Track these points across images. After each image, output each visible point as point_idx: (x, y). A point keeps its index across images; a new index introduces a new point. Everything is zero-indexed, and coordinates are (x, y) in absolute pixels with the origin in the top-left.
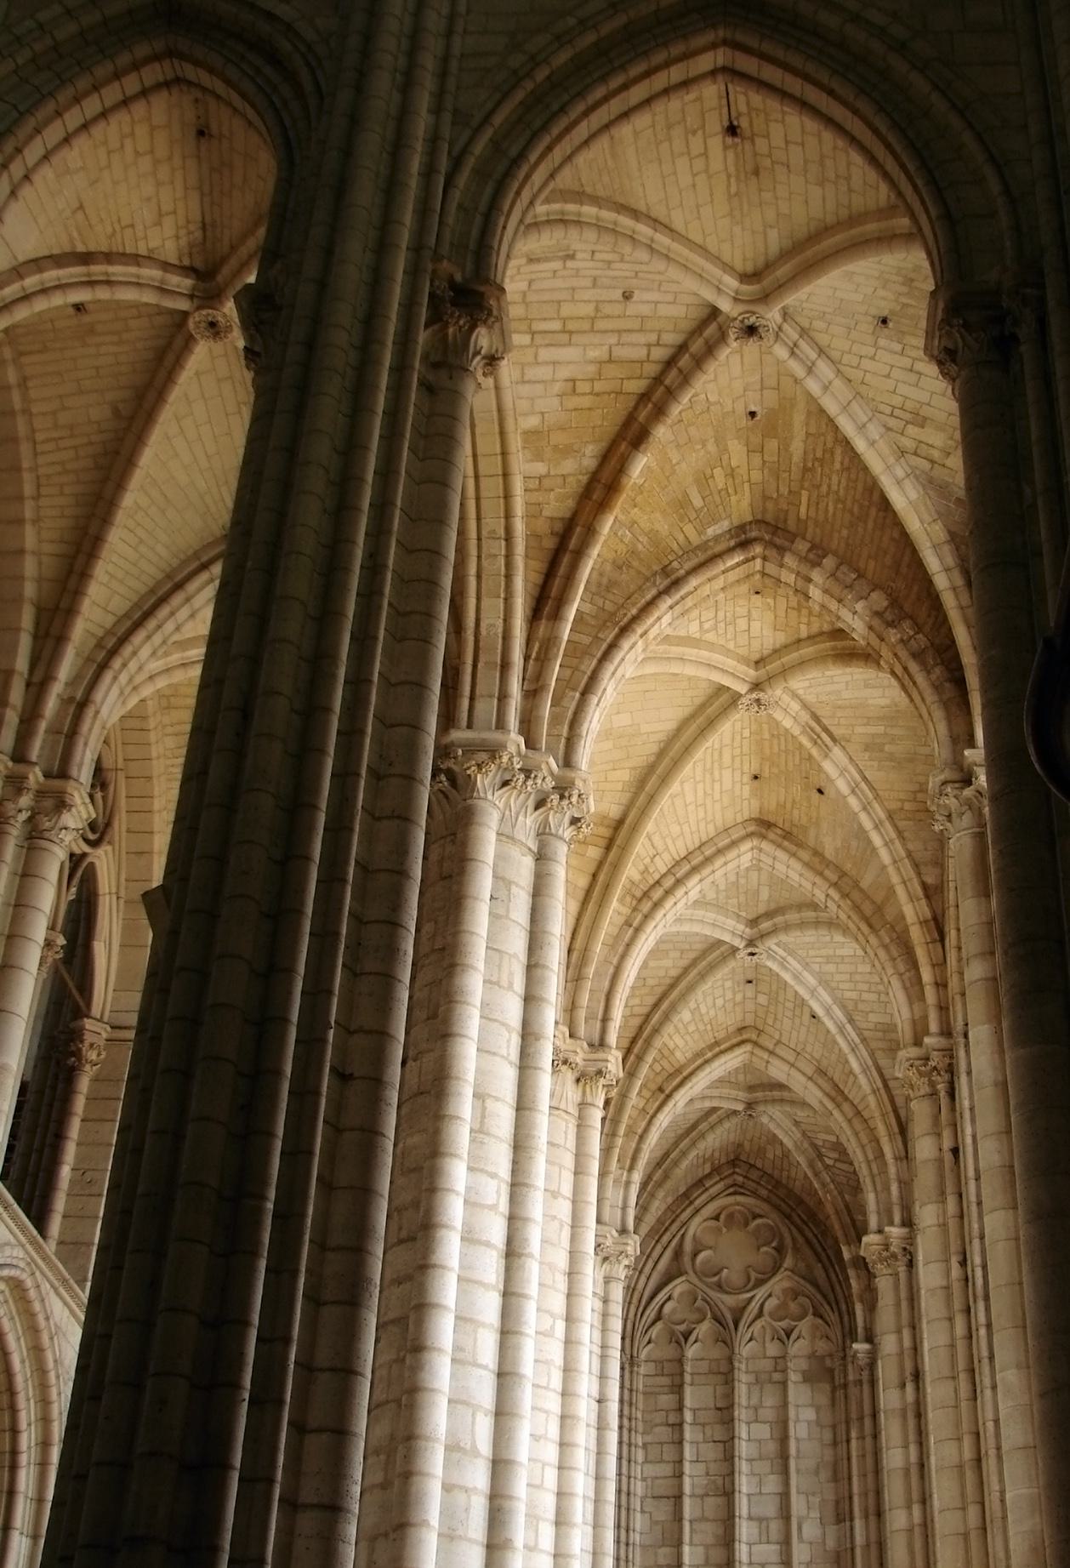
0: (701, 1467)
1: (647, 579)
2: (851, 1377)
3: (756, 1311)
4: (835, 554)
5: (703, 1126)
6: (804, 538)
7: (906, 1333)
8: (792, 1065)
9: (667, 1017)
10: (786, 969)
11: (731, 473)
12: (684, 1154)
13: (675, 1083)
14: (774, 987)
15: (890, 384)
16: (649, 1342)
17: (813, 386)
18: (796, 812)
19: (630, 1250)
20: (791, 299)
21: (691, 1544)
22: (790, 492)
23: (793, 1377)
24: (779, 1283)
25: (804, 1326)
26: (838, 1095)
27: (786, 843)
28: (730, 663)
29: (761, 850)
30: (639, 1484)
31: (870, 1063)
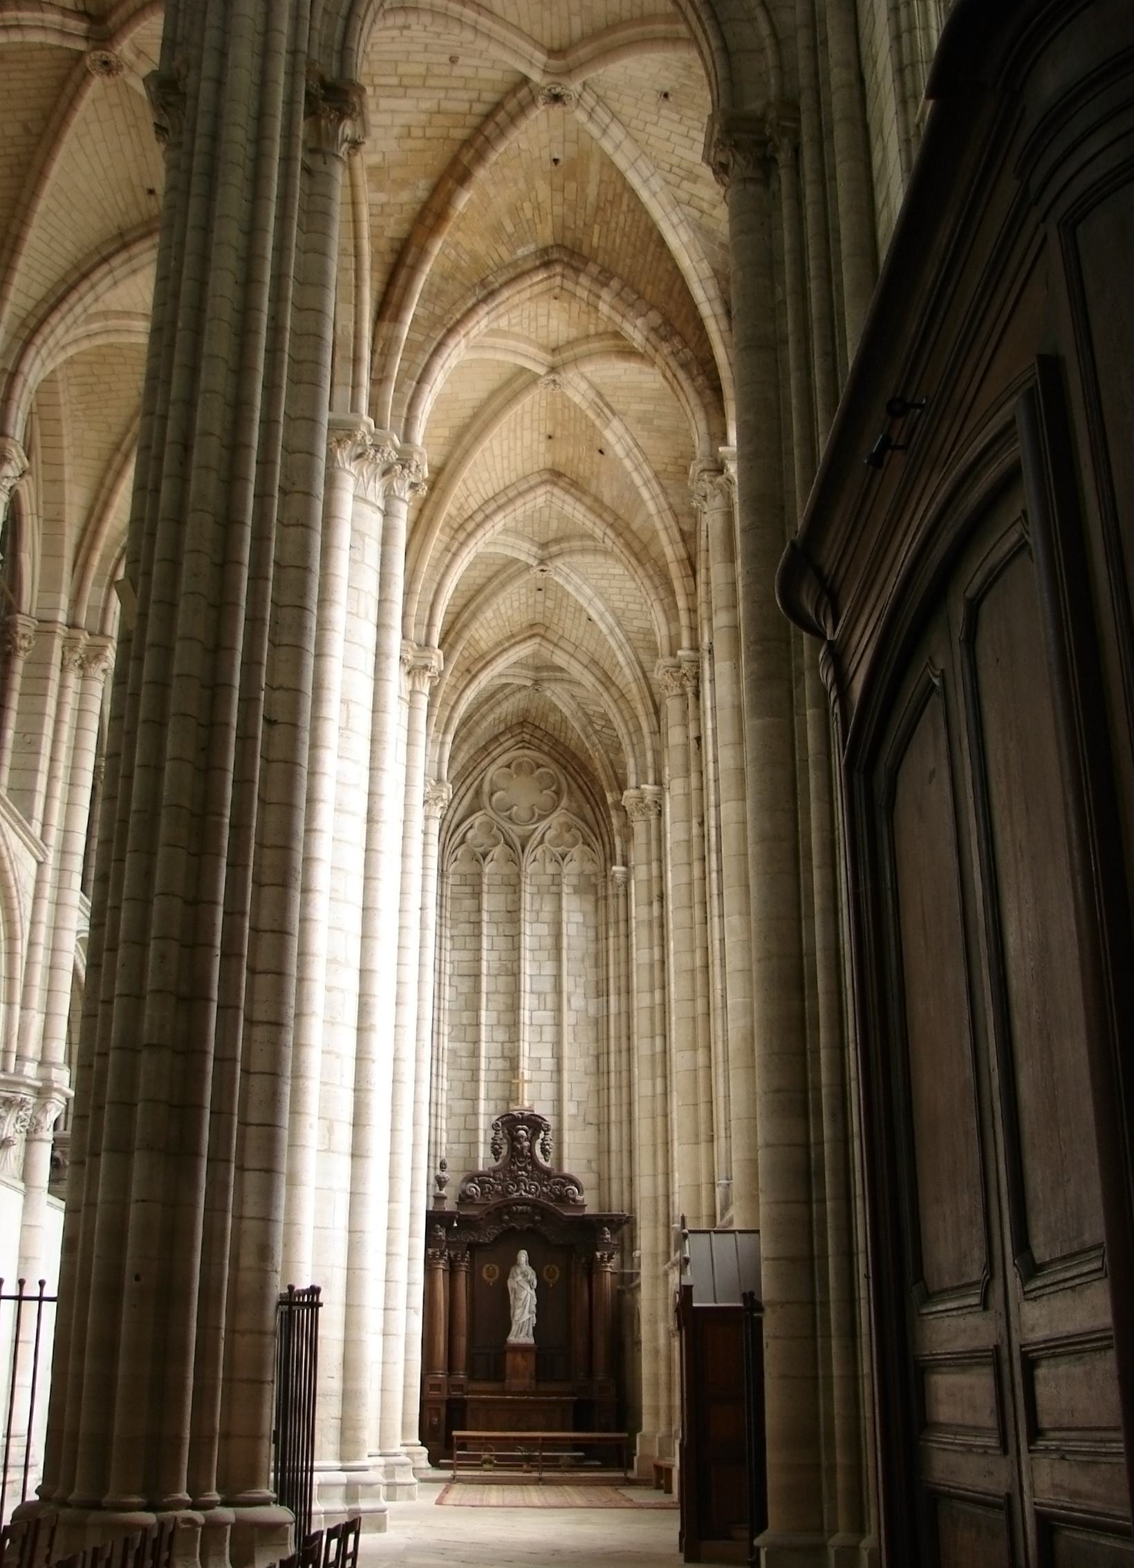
0: (495, 955)
1: (469, 289)
2: (610, 892)
3: (538, 839)
4: (621, 278)
5: (500, 696)
6: (595, 263)
8: (572, 656)
9: (474, 616)
10: (569, 582)
11: (538, 207)
12: (484, 717)
13: (481, 665)
14: (560, 595)
15: (669, 147)
16: (455, 860)
17: (608, 146)
18: (581, 467)
19: (445, 796)
20: (590, 75)
21: (487, 1010)
22: (585, 224)
23: (566, 889)
24: (557, 819)
25: (576, 852)
26: (607, 681)
27: (573, 490)
28: (532, 351)
29: (553, 494)
30: (448, 965)
31: (633, 658)
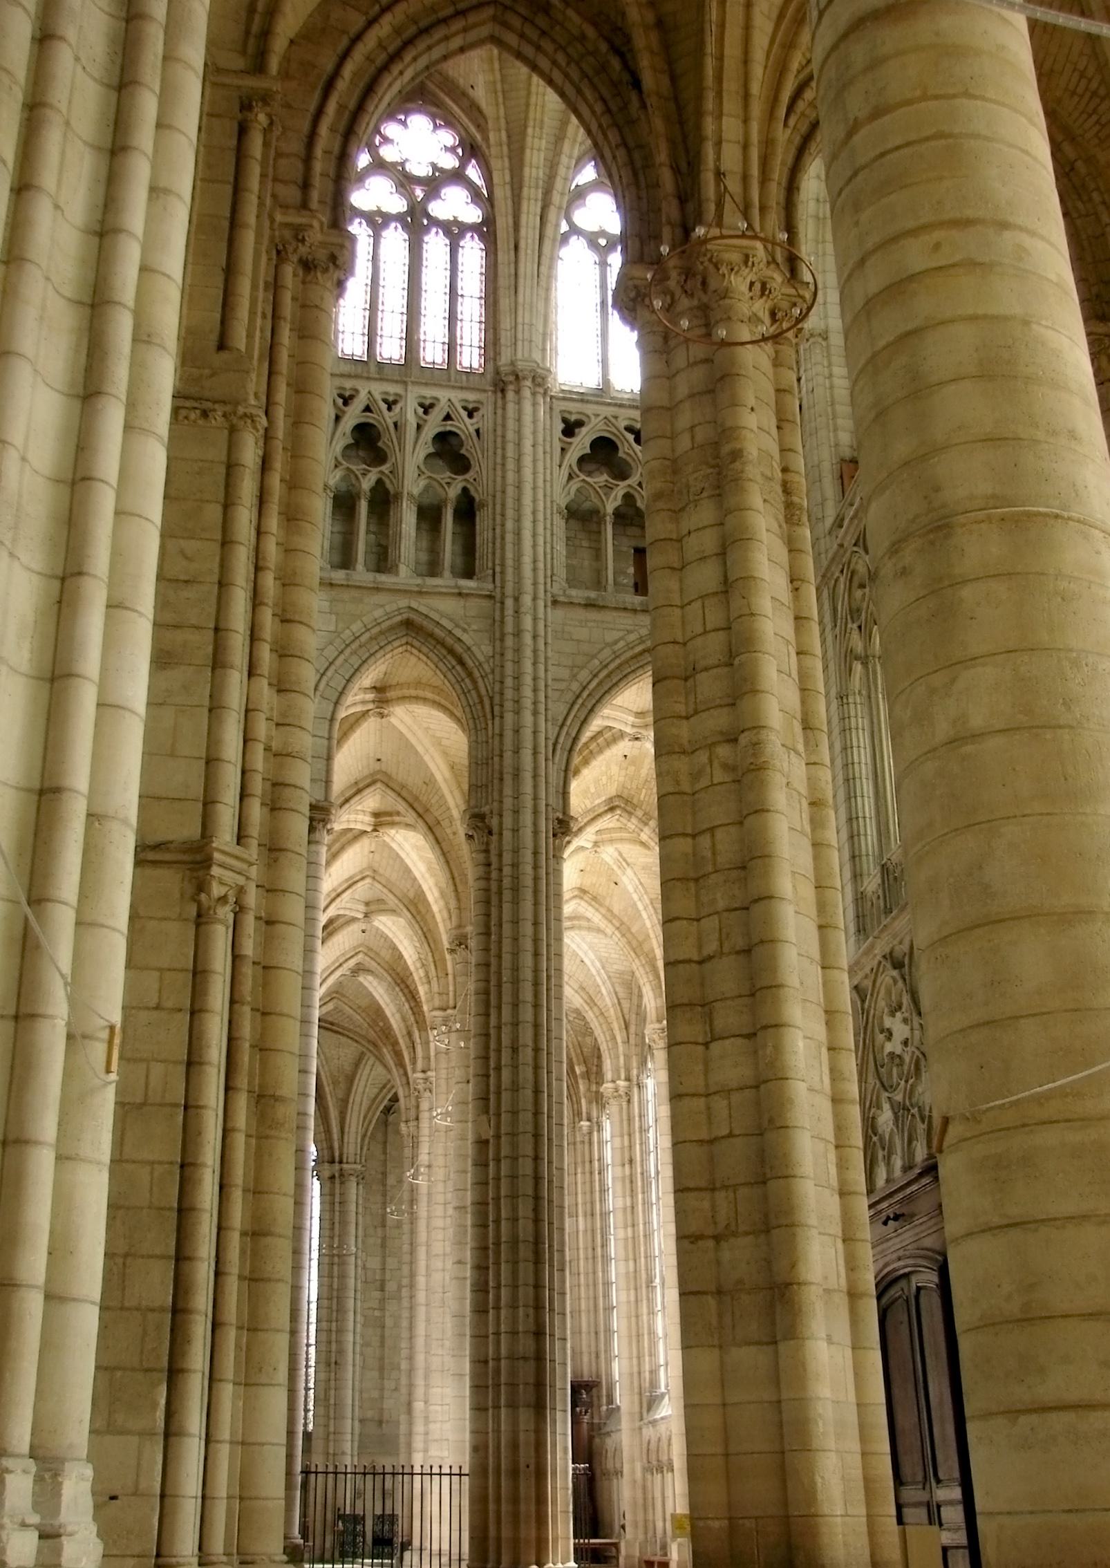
2: (578, 1139)
7: (626, 1138)
26: (591, 1002)
